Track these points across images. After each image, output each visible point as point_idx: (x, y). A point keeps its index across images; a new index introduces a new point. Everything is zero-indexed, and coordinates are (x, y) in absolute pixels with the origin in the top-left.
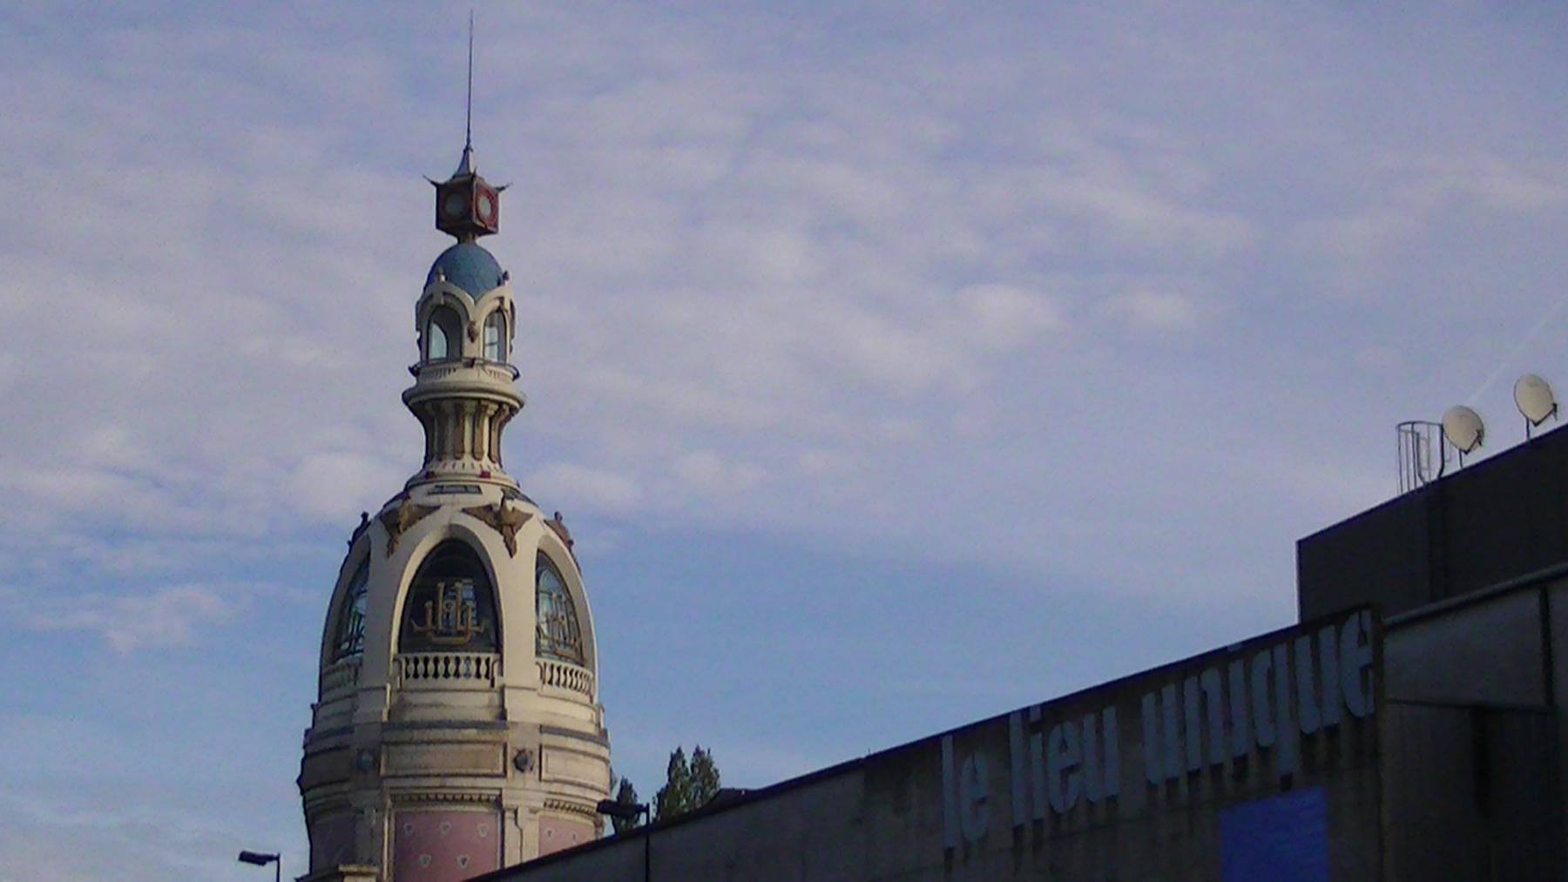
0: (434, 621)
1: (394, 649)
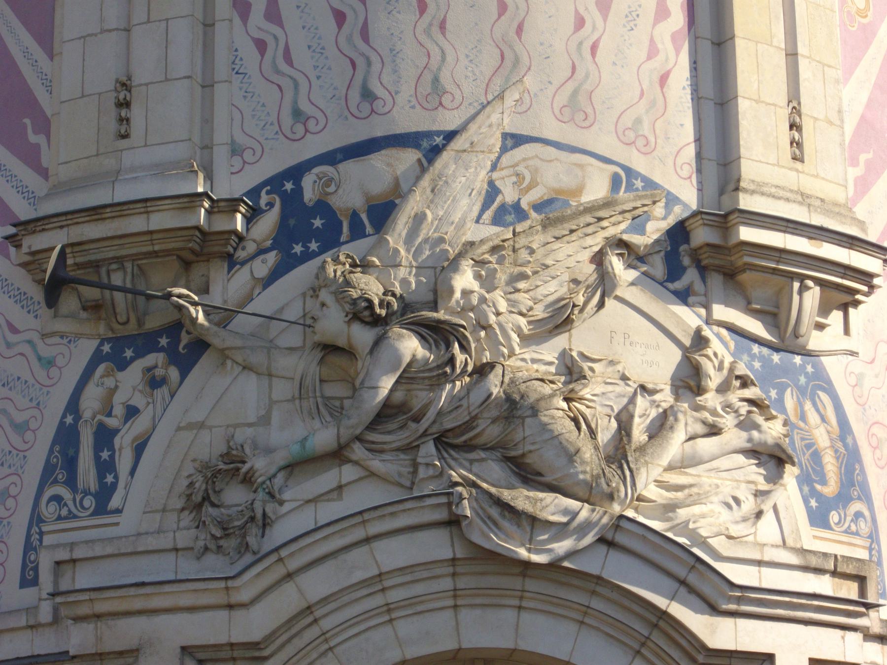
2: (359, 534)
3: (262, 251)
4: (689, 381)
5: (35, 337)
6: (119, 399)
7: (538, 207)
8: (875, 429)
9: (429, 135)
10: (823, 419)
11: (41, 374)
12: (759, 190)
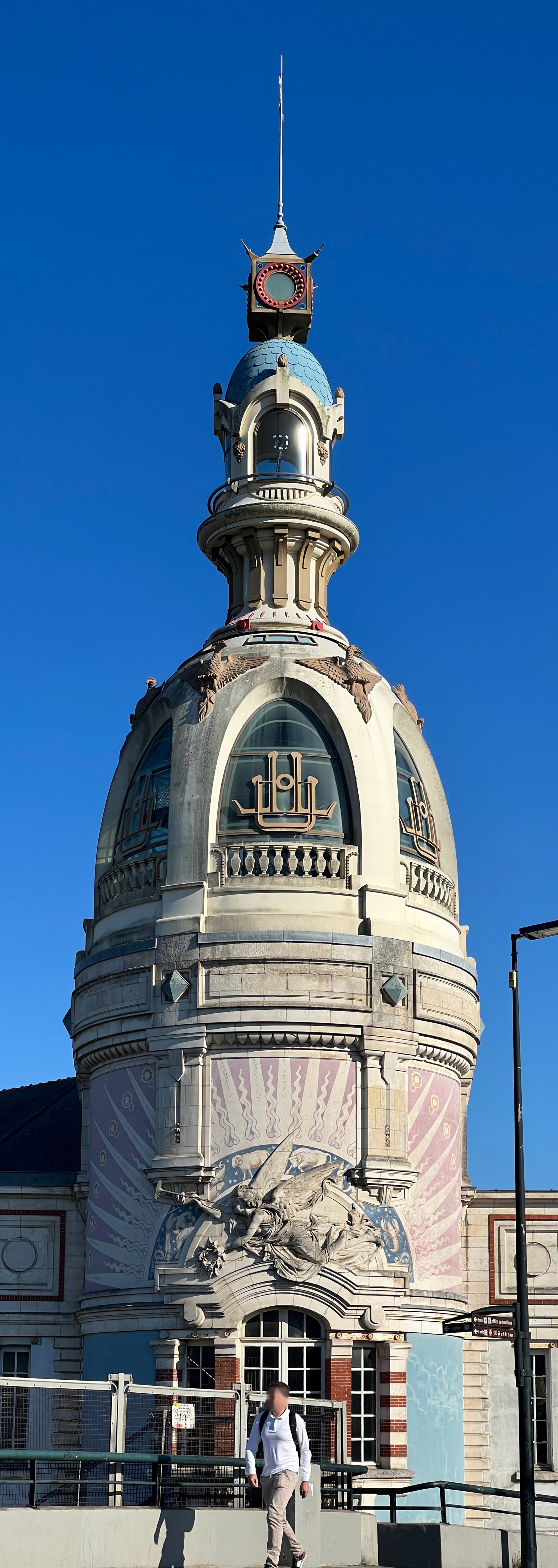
0: (267, 802)
1: (212, 839)
2: (248, 1273)
3: (219, 1182)
5: (151, 1202)
6: (177, 1225)
7: (303, 1168)
8: (414, 1228)
9: (270, 1146)
10: (394, 1228)
11: (154, 1214)
12: (374, 1158)
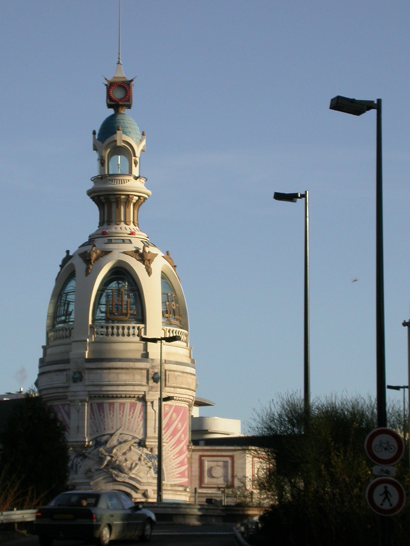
1: (90, 323)
4: (140, 459)
